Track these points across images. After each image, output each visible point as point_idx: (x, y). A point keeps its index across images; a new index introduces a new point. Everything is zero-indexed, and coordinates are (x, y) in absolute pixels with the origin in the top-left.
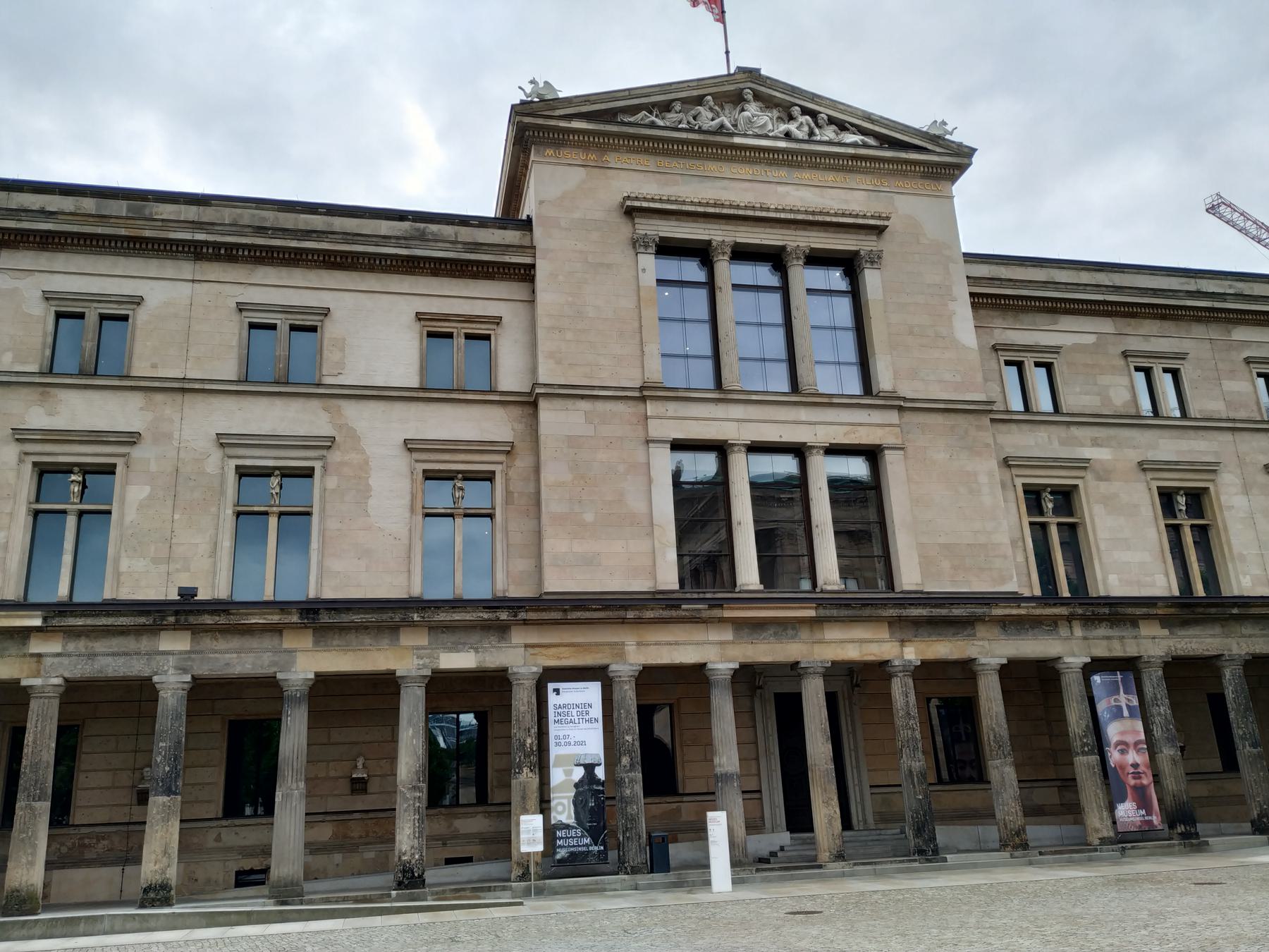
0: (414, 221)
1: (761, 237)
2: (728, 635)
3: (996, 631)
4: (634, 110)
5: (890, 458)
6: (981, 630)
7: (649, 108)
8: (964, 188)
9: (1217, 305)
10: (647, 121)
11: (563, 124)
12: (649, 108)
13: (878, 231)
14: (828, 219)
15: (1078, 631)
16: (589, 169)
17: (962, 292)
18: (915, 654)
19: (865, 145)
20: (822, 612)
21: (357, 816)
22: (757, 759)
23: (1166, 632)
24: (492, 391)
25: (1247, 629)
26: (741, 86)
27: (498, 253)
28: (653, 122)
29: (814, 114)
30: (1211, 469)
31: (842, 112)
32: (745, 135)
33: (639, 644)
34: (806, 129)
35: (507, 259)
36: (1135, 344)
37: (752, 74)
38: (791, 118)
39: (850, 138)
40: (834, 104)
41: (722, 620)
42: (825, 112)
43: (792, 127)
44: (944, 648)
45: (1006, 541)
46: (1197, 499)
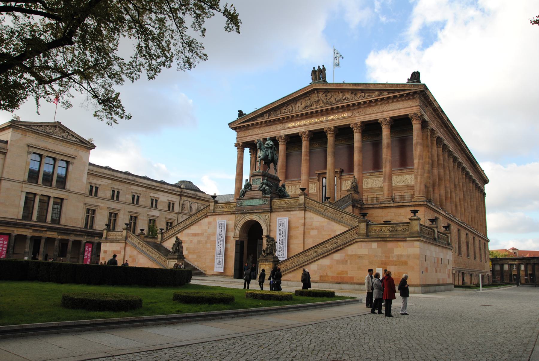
2: (31, 231)
3: (74, 235)
5: (65, 201)
6: (71, 235)
7: (37, 126)
8: (92, 151)
9: (130, 182)
10: (37, 129)
12: (37, 126)
15: (86, 237)
17: (86, 172)
20: (48, 230)
29: (69, 133)
30: (119, 210)
31: (74, 134)
32: (55, 135)
33: (17, 231)
34: (66, 136)
37: (59, 123)
38: (64, 132)
41: (32, 229)
42: (71, 133)
43: (64, 135)
45: (81, 218)
46: (116, 215)
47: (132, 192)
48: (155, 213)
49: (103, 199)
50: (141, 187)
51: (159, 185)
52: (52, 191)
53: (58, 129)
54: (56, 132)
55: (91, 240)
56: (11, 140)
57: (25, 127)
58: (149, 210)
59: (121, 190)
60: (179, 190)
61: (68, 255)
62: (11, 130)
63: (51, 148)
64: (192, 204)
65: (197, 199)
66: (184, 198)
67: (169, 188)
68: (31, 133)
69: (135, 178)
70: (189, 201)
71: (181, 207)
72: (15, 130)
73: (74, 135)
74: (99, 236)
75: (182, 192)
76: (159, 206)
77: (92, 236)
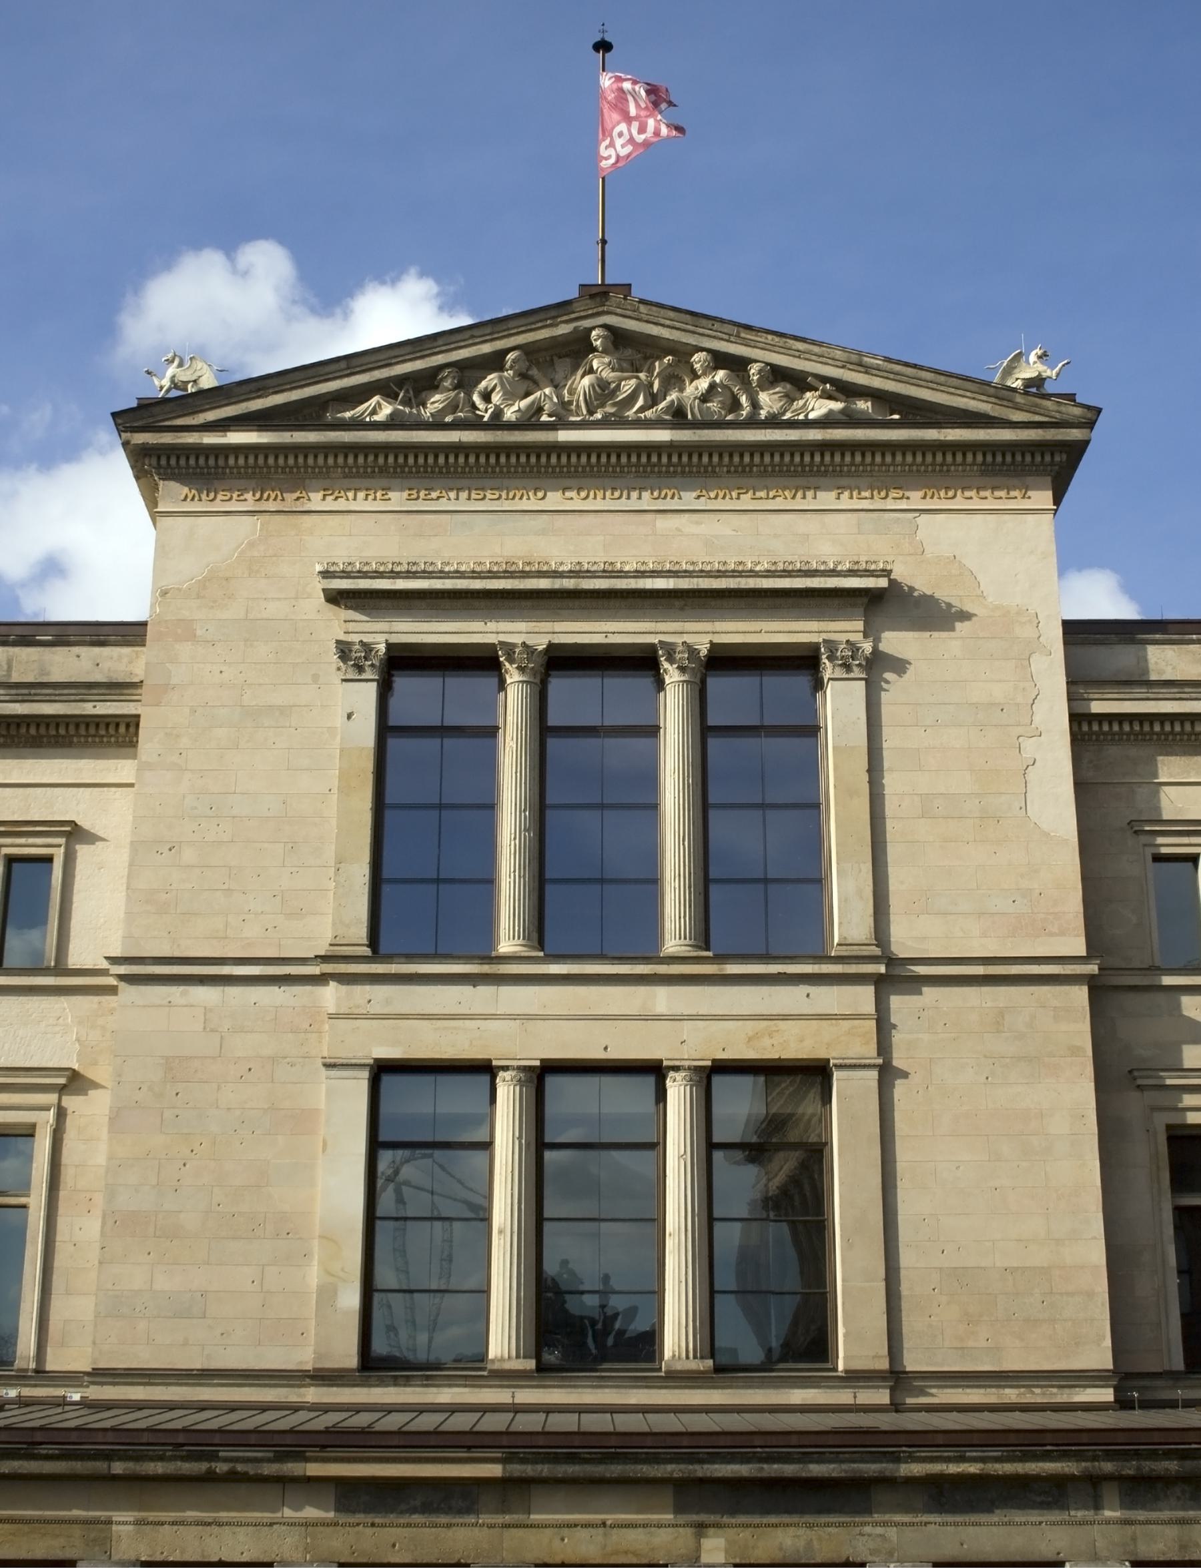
1: (605, 629)
13: (865, 600)
14: (752, 583)
16: (267, 517)
18: (726, 1552)
24: (60, 969)
27: (72, 698)
35: (88, 709)
52: (662, 999)
54: (604, 392)
56: (164, 593)
57: (261, 428)
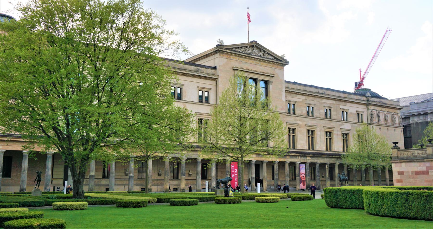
0: (197, 67)
2: (255, 156)
4: (236, 48)
6: (287, 157)
7: (238, 48)
8: (286, 67)
9: (321, 95)
10: (238, 51)
11: (225, 50)
12: (238, 48)
15: (299, 158)
17: (284, 89)
19: (272, 59)
21: (190, 180)
22: (248, 174)
23: (310, 159)
25: (321, 159)
26: (254, 45)
28: (239, 51)
29: (264, 51)
30: (316, 127)
32: (254, 55)
36: (308, 102)
37: (256, 42)
38: (261, 51)
39: (271, 57)
40: (268, 50)
43: (260, 54)
44: (282, 160)
47: (324, 106)
48: (347, 126)
49: (300, 116)
50: (331, 100)
51: (346, 95)
53: (255, 48)
55: (304, 160)
56: (220, 66)
58: (341, 123)
59: (314, 105)
60: (365, 99)
61: (287, 178)
62: (217, 55)
63: (253, 69)
64: (379, 112)
65: (384, 107)
66: (371, 108)
67: (356, 98)
68: (234, 56)
69: (325, 91)
70: (376, 110)
71: (369, 118)
72: (221, 55)
73: (269, 53)
74: (311, 155)
75: (368, 101)
76: (350, 119)
77: (304, 156)
